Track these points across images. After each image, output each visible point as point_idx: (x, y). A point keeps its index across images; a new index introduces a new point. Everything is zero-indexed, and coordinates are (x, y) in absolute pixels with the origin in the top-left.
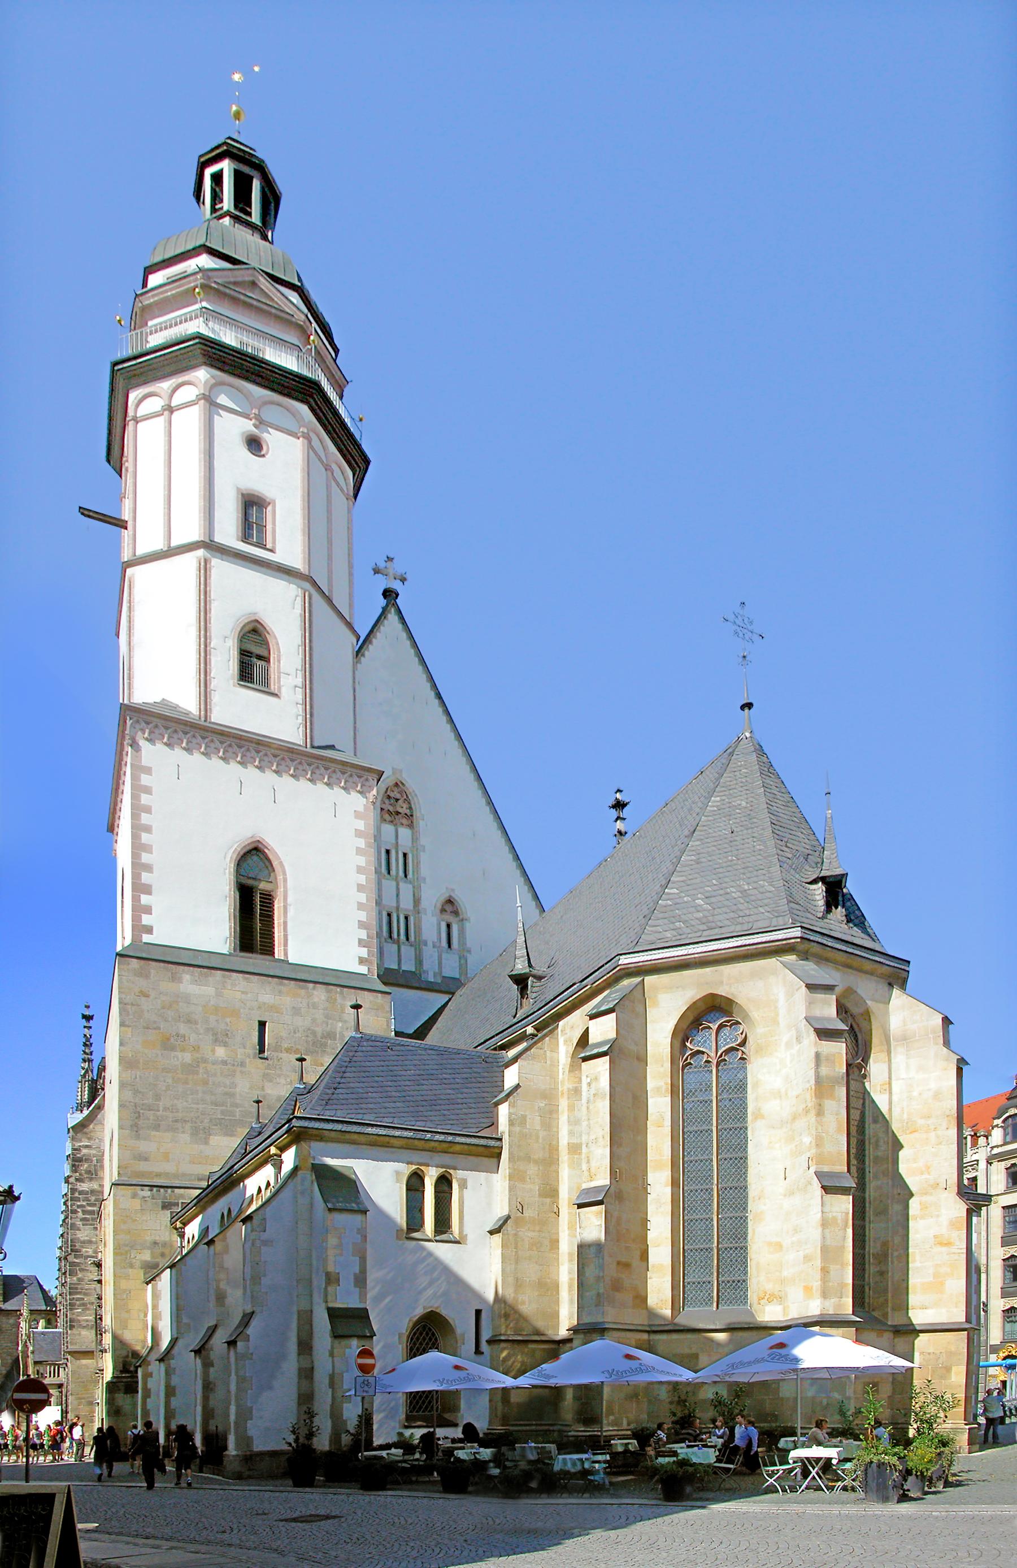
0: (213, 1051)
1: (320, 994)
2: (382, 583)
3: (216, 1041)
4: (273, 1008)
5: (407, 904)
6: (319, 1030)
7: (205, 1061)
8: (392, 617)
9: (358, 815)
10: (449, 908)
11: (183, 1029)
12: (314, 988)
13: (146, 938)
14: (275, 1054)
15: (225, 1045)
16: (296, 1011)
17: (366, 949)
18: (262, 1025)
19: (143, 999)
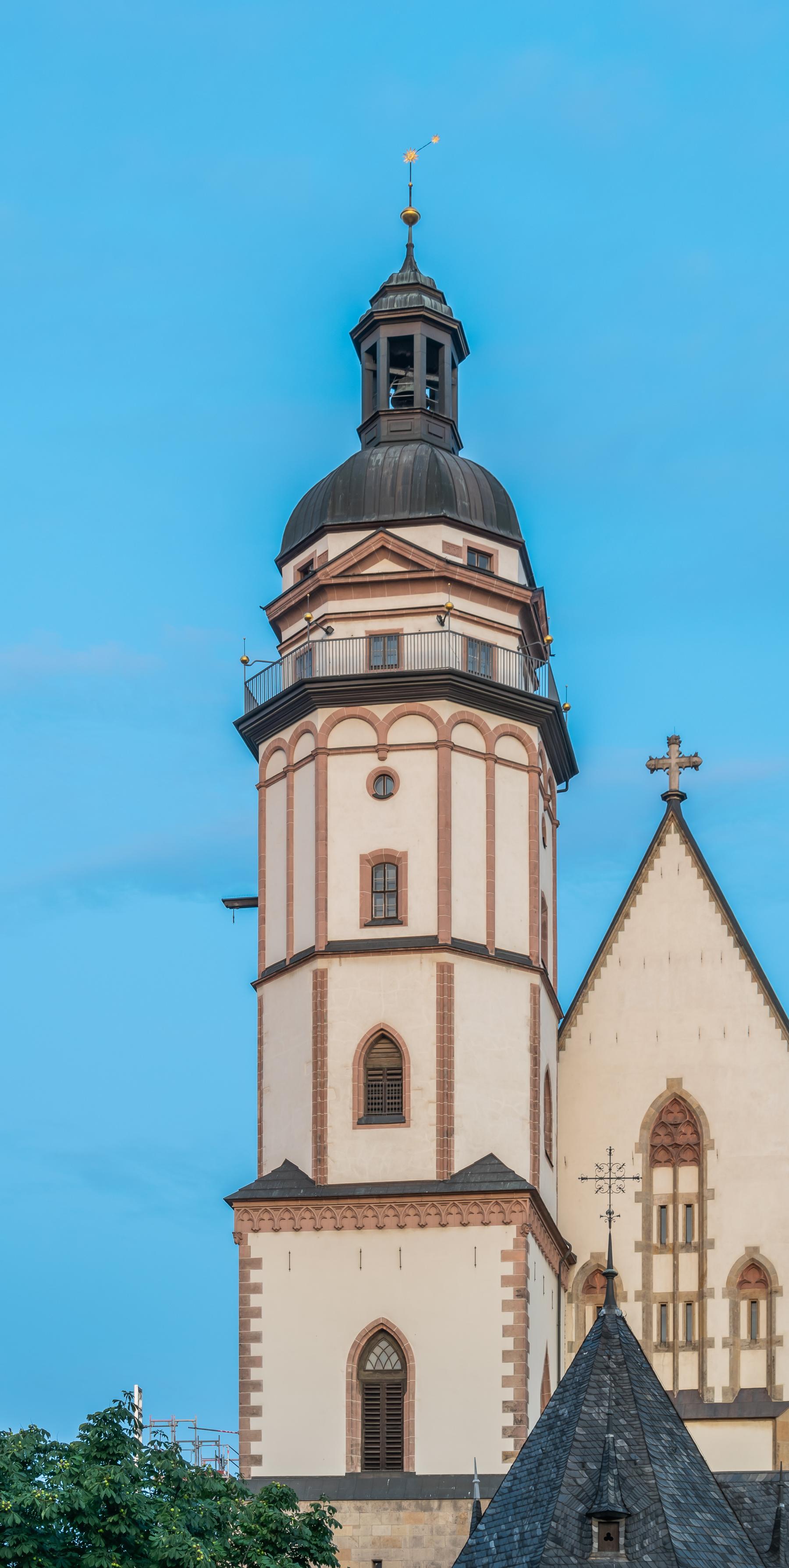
5: (688, 1284)
10: (753, 1276)
17: (512, 1440)
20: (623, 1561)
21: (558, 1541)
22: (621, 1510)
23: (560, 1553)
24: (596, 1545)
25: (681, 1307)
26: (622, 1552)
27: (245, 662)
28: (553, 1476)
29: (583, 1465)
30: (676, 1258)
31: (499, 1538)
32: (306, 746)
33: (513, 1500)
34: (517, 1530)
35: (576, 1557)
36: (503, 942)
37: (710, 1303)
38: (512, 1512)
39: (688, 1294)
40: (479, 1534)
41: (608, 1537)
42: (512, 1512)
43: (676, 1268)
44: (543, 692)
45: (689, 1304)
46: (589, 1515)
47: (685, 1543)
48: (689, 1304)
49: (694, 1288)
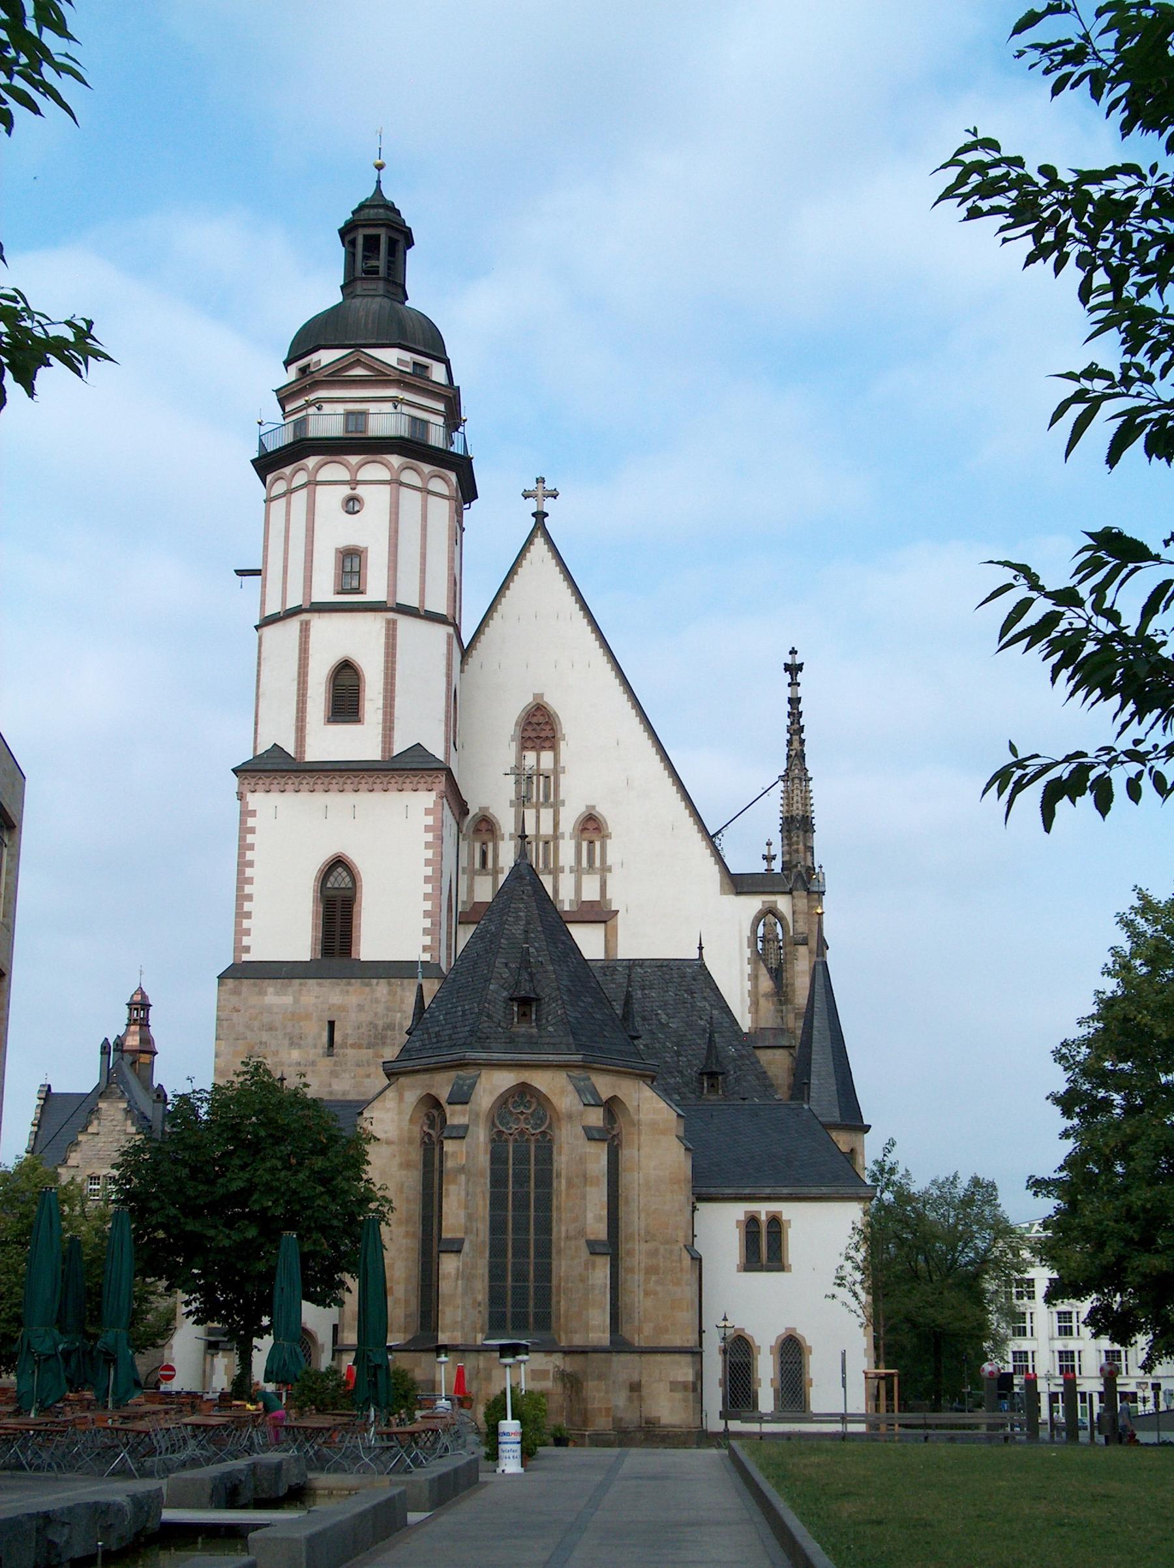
0: (289, 1054)
1: (381, 988)
2: (532, 505)
3: (292, 1044)
4: (342, 1008)
5: (546, 829)
6: (380, 1023)
7: (282, 1064)
8: (539, 542)
9: (428, 812)
11: (265, 1036)
12: (377, 984)
13: (246, 957)
14: (342, 1051)
15: (299, 1046)
16: (360, 1008)
18: (332, 1024)
19: (235, 1014)
20: (535, 1030)
21: (489, 1016)
22: (533, 996)
23: (491, 1024)
24: (516, 1020)
25: (541, 845)
26: (534, 1024)
27: (260, 423)
28: (486, 972)
29: (506, 965)
30: (538, 812)
31: (446, 1014)
32: (301, 478)
33: (457, 987)
34: (459, 1008)
35: (502, 1028)
36: (431, 606)
37: (561, 842)
38: (456, 996)
39: (546, 836)
40: (432, 1010)
41: (524, 1014)
42: (456, 996)
43: (538, 818)
44: (457, 449)
45: (547, 843)
46: (511, 999)
47: (576, 1018)
48: (547, 843)
49: (551, 832)
